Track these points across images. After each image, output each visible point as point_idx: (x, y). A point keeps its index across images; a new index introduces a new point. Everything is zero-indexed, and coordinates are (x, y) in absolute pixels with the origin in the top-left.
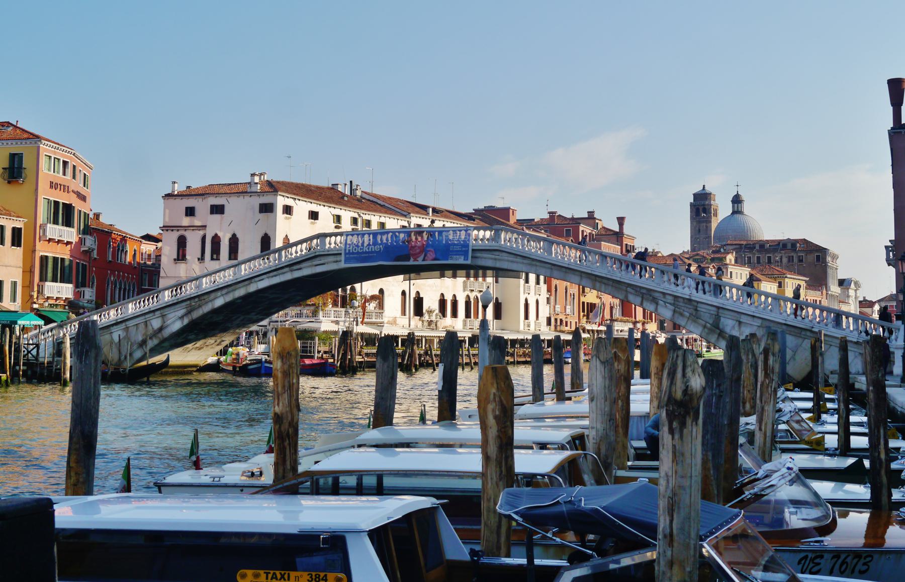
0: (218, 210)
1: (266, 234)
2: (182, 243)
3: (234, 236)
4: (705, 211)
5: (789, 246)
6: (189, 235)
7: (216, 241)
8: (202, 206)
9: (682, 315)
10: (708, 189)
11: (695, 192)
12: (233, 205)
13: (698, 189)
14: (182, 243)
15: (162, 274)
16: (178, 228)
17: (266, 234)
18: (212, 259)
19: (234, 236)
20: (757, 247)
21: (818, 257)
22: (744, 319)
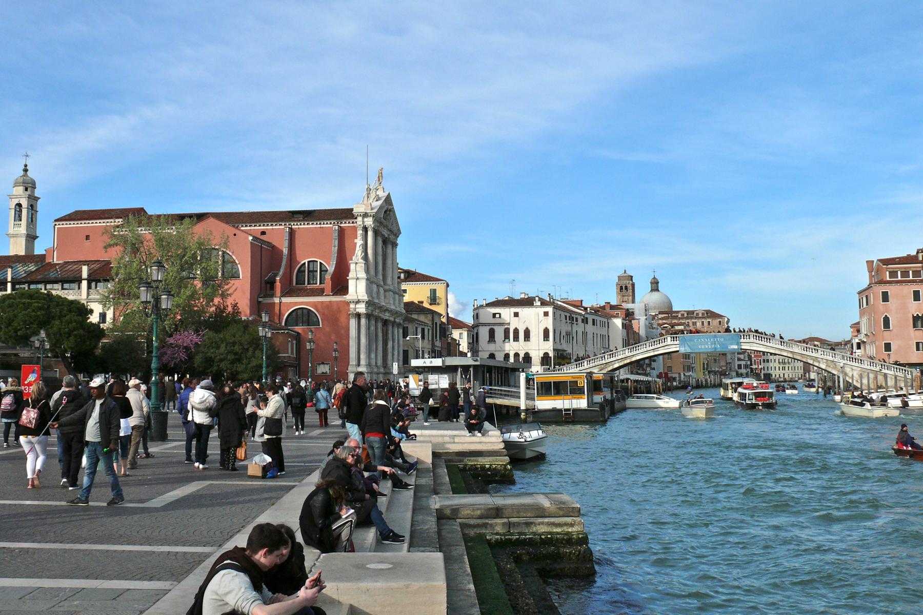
0: (516, 315)
1: (546, 328)
2: (492, 334)
3: (527, 328)
4: (626, 288)
5: (700, 315)
6: (495, 327)
7: (516, 331)
8: (506, 313)
9: (829, 367)
10: (629, 273)
11: (619, 275)
12: (524, 311)
13: (621, 273)
14: (492, 334)
15: (480, 349)
16: (489, 324)
17: (546, 328)
18: (514, 341)
19: (527, 328)
20: (680, 316)
21: (720, 322)
22: (854, 368)
